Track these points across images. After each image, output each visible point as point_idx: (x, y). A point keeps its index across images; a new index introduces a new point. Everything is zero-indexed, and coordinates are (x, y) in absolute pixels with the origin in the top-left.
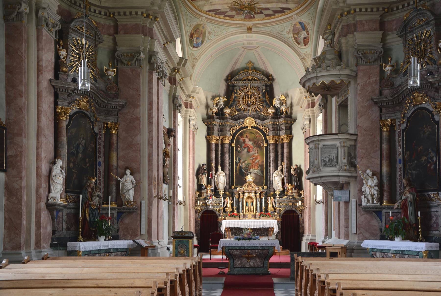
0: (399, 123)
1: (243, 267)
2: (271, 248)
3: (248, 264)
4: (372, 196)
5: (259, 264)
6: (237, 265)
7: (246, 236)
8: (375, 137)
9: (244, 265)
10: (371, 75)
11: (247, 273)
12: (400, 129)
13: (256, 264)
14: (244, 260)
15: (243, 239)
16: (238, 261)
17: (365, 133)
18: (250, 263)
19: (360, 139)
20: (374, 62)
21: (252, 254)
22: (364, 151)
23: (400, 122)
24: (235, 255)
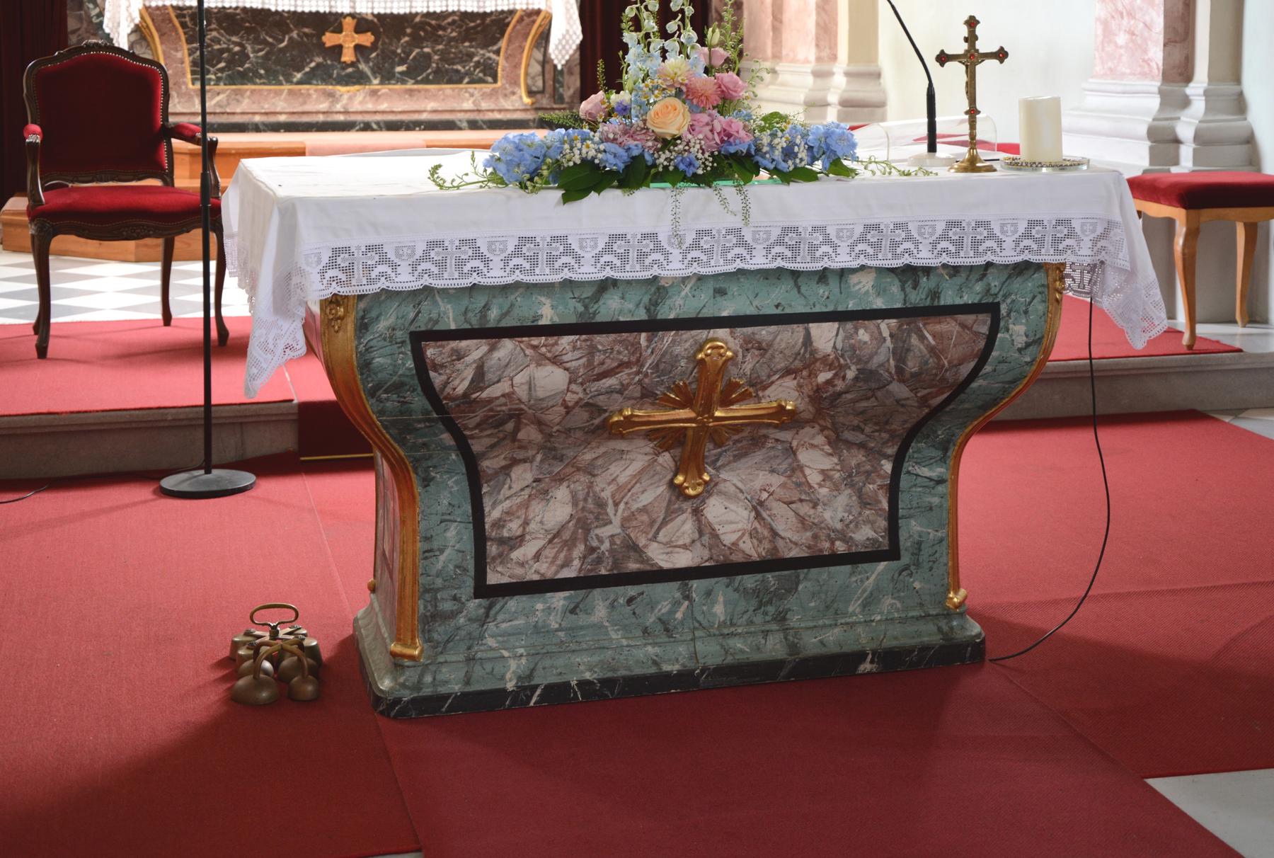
1: (620, 579)
2: (1024, 288)
3: (684, 526)
5: (836, 509)
6: (528, 560)
7: (672, 119)
9: (633, 548)
11: (674, 658)
13: (784, 521)
14: (632, 477)
15: (634, 175)
16: (541, 490)
18: (715, 510)
21: (758, 385)
24: (510, 419)
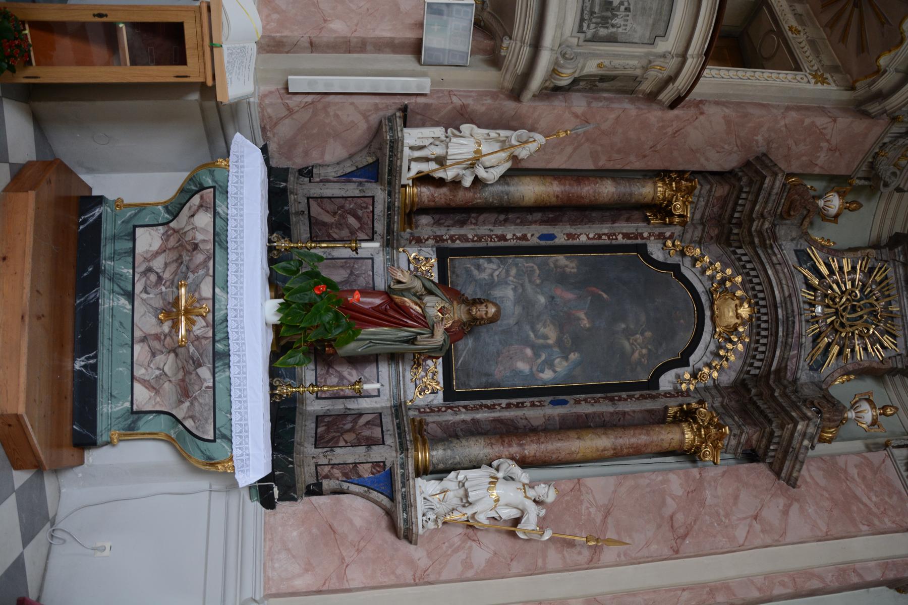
0: (668, 234)
4: (441, 161)
8: (645, 156)
10: (837, 154)
12: (648, 238)
17: (670, 130)
19: (655, 115)
20: (872, 166)
22: (605, 126)
23: (671, 237)
